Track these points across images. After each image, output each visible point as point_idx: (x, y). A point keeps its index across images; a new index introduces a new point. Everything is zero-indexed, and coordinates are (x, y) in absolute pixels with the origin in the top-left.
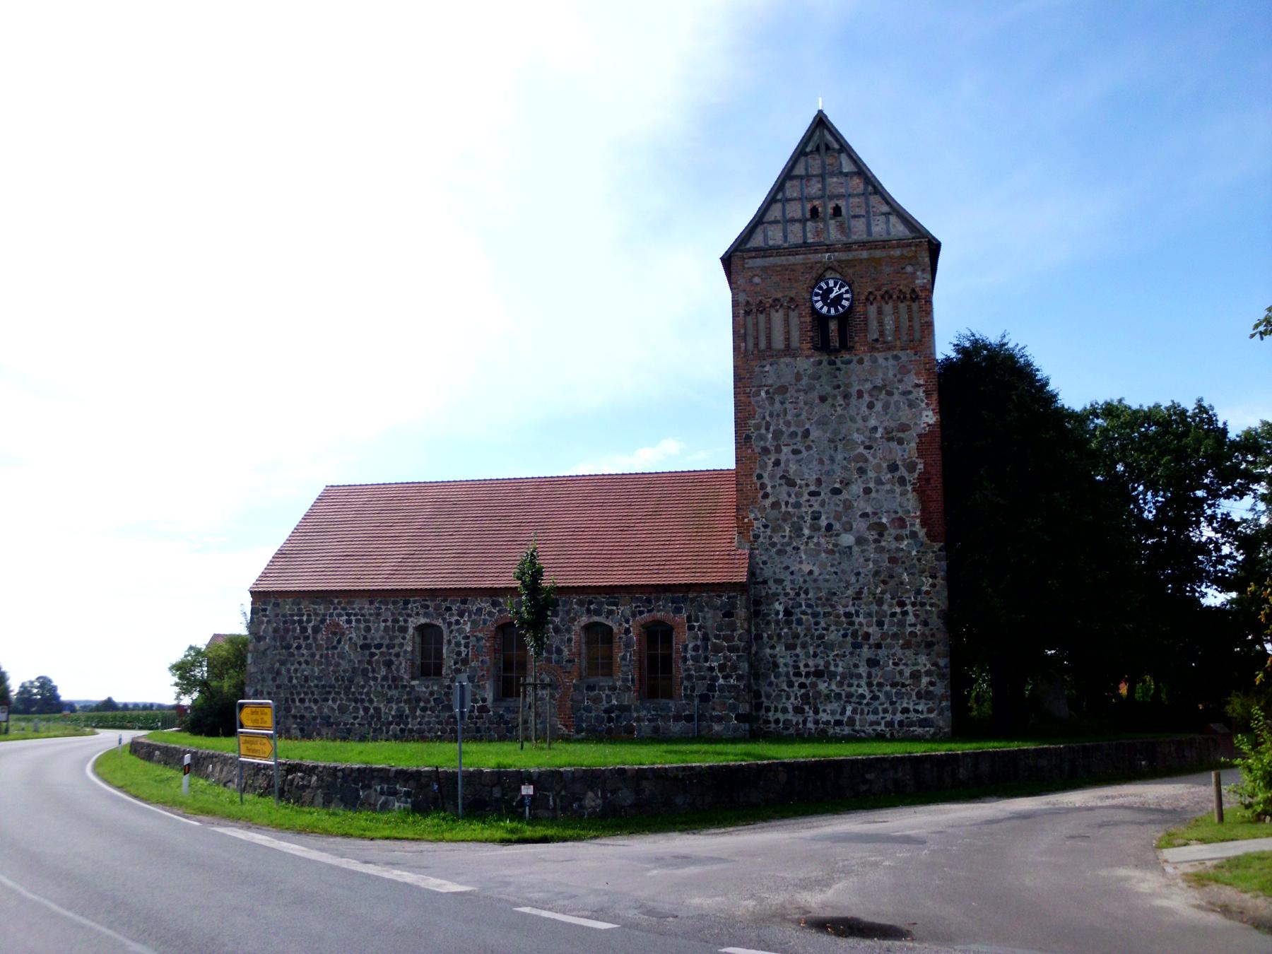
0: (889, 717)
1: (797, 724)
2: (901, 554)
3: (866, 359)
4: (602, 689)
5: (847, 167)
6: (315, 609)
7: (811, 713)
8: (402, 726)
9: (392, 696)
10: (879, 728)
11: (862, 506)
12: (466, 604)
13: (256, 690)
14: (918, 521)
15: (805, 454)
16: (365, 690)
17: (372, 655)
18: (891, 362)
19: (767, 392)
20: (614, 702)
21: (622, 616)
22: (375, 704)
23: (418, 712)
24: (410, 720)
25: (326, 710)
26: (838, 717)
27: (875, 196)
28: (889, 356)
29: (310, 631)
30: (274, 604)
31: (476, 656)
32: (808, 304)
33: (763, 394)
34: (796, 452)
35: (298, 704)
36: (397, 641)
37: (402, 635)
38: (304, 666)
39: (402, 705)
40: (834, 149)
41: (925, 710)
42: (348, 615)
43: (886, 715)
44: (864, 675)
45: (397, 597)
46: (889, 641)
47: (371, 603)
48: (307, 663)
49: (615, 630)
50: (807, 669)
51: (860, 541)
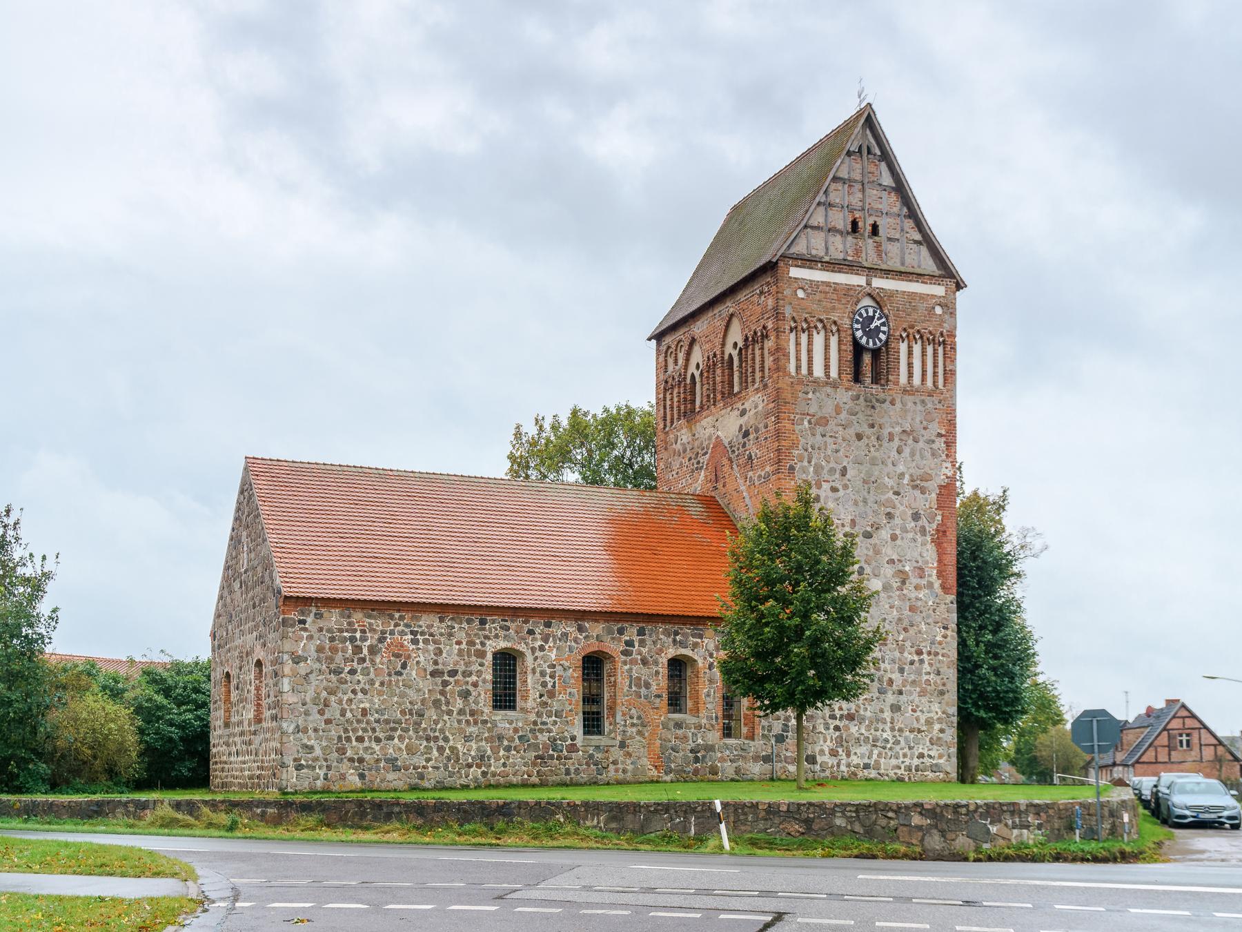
0: (908, 761)
1: (832, 767)
2: (919, 603)
3: (898, 401)
4: (688, 727)
5: (887, 180)
6: (370, 624)
7: (844, 757)
8: (483, 768)
9: (471, 733)
10: (899, 772)
11: (889, 552)
12: (550, 627)
13: (298, 726)
14: (935, 572)
15: (841, 493)
16: (439, 726)
17: (445, 683)
18: (919, 407)
19: (810, 422)
20: (700, 741)
21: (707, 650)
22: (451, 743)
23: (502, 753)
24: (492, 761)
25: (391, 751)
26: (866, 761)
27: (909, 220)
28: (917, 401)
29: (365, 651)
30: (316, 614)
31: (565, 687)
32: (850, 332)
33: (806, 423)
34: (834, 490)
35: (354, 743)
36: (475, 667)
37: (479, 660)
38: (360, 695)
39: (484, 743)
40: (875, 155)
41: (937, 755)
42: (412, 633)
43: (905, 760)
44: (888, 720)
45: (472, 614)
46: (908, 688)
47: (441, 620)
48: (364, 692)
49: (700, 665)
50: (841, 712)
51: (887, 587)
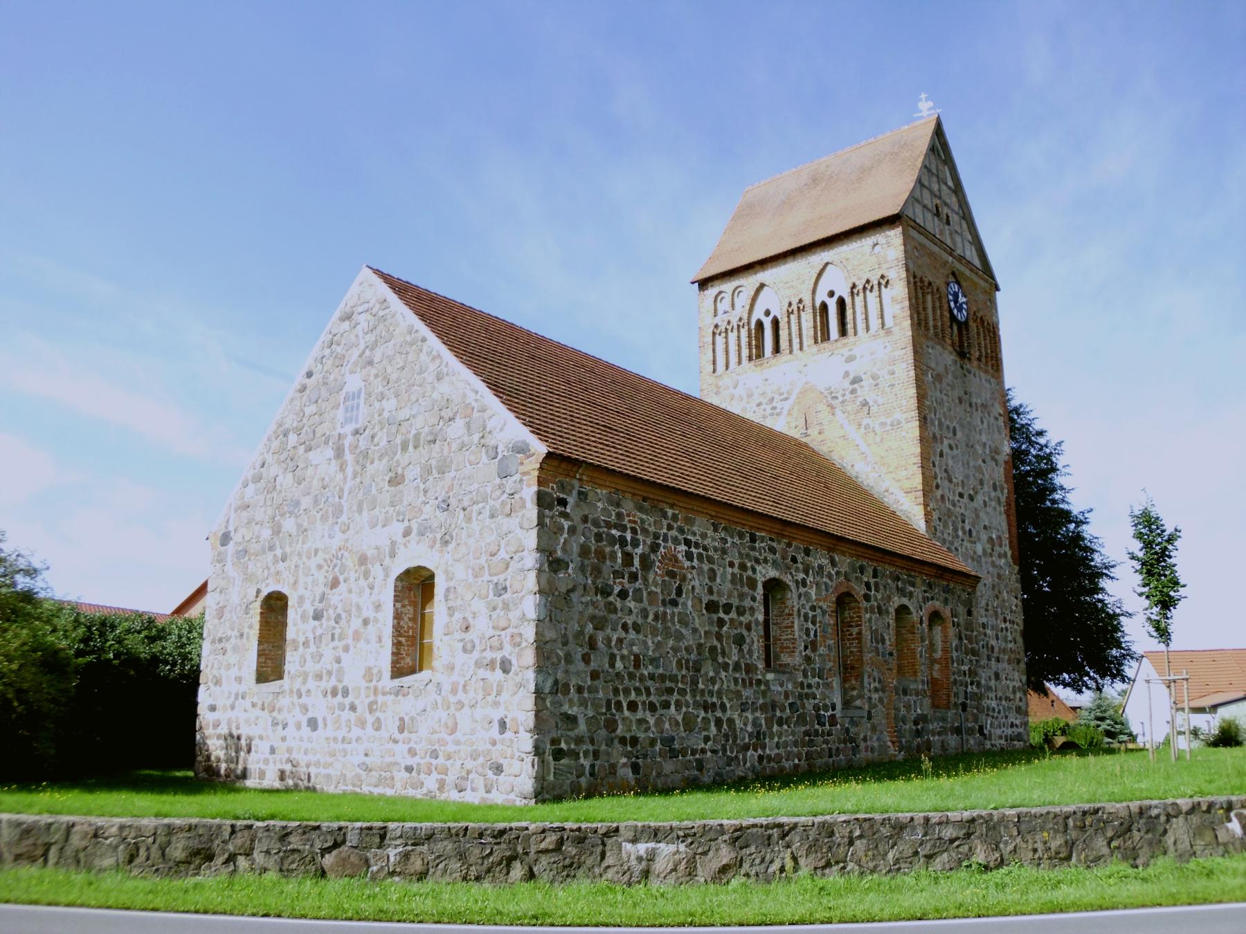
6: (642, 521)
13: (556, 682)
16: (716, 687)
17: (721, 623)
23: (775, 728)
24: (767, 740)
29: (637, 562)
38: (632, 635)
48: (636, 627)
